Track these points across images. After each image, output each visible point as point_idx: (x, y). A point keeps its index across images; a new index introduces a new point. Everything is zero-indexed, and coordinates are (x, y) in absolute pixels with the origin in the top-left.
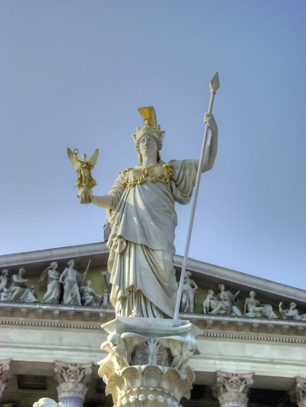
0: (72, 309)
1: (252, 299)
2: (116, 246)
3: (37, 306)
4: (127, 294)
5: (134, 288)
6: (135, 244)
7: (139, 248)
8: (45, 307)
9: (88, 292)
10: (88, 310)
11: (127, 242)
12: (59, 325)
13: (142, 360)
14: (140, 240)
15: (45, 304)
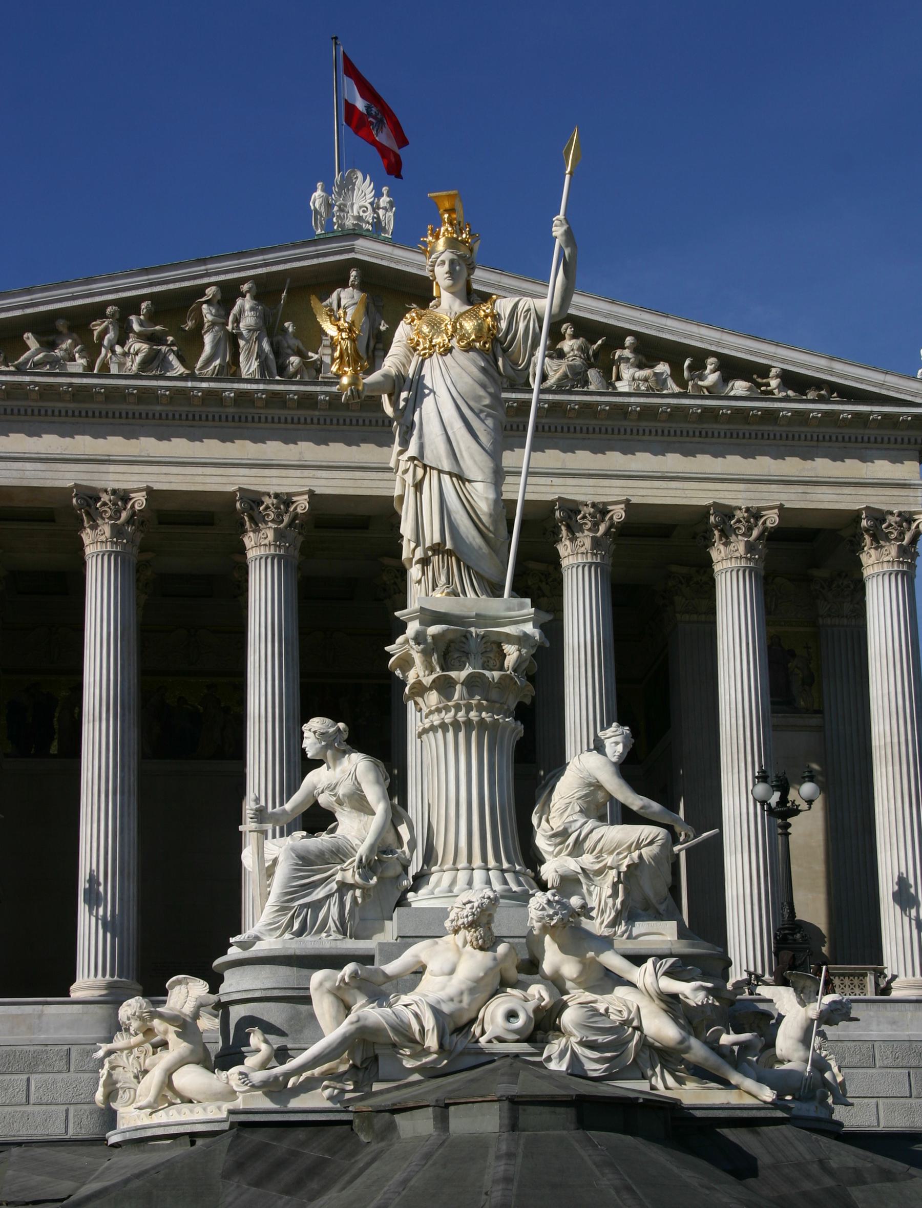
0: (261, 387)
1: (627, 353)
2: (406, 471)
3: (189, 384)
4: (430, 553)
5: (442, 546)
6: (440, 472)
7: (446, 478)
8: (204, 385)
9: (289, 347)
10: (294, 388)
11: (425, 467)
12: (237, 418)
13: (459, 661)
14: (446, 465)
15: (203, 380)
